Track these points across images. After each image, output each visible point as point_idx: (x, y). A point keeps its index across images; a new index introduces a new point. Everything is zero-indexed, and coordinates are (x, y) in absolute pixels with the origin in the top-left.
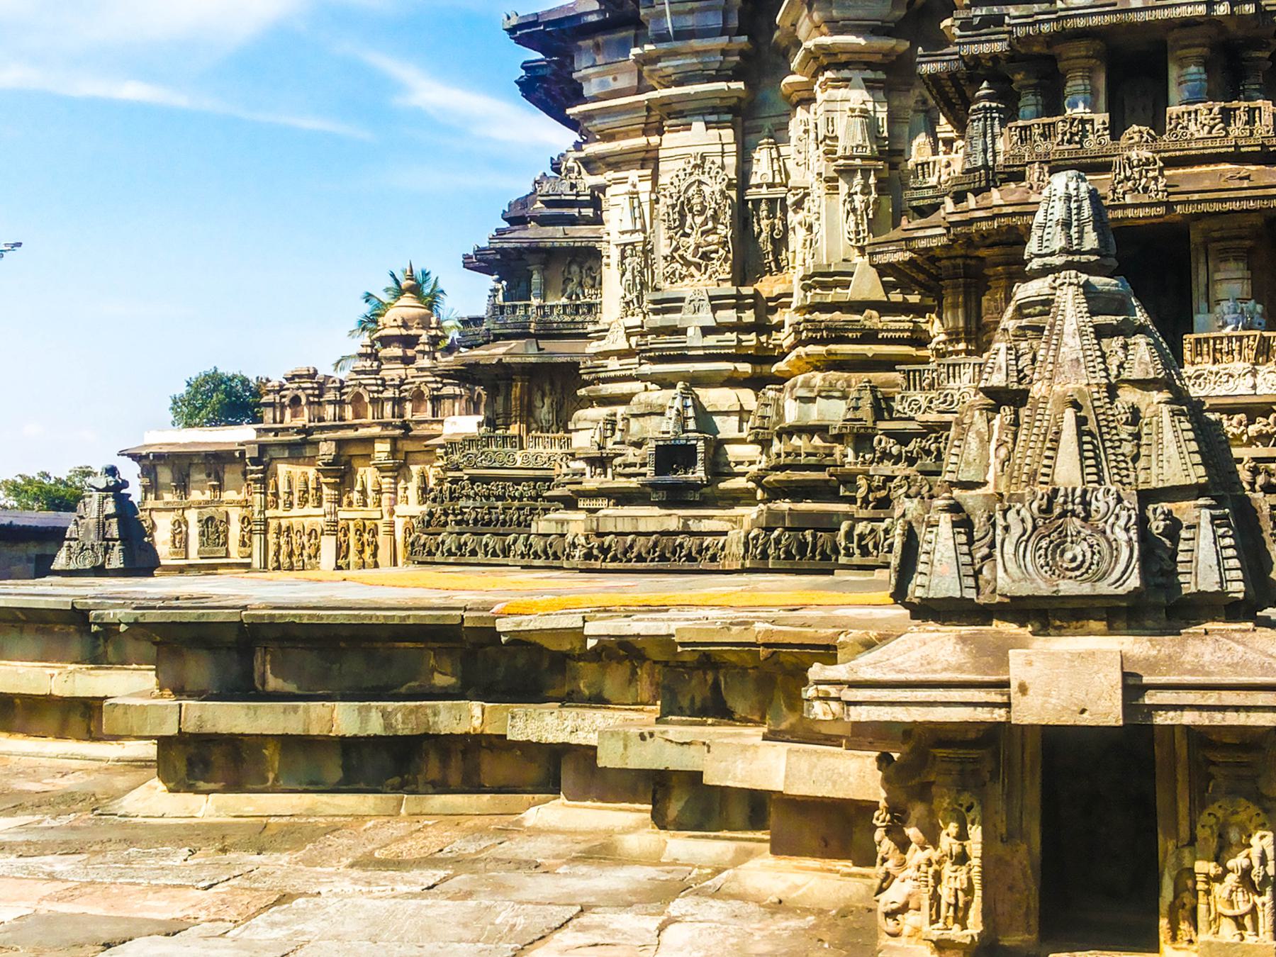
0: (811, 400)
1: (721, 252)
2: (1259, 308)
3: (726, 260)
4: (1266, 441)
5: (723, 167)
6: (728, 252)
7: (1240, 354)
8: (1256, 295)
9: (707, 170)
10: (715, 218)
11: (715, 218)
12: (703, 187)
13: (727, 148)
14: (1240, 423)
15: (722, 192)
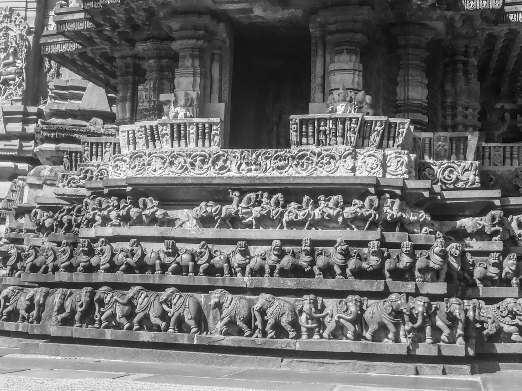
0: (40, 187)
1: (17, 80)
2: (368, 98)
3: (20, 86)
4: (361, 224)
5: (25, 19)
6: (23, 80)
7: (343, 136)
8: (367, 88)
9: (13, 19)
10: (15, 54)
11: (15, 54)
12: (10, 32)
13: (30, 5)
14: (337, 205)
15: (21, 36)
